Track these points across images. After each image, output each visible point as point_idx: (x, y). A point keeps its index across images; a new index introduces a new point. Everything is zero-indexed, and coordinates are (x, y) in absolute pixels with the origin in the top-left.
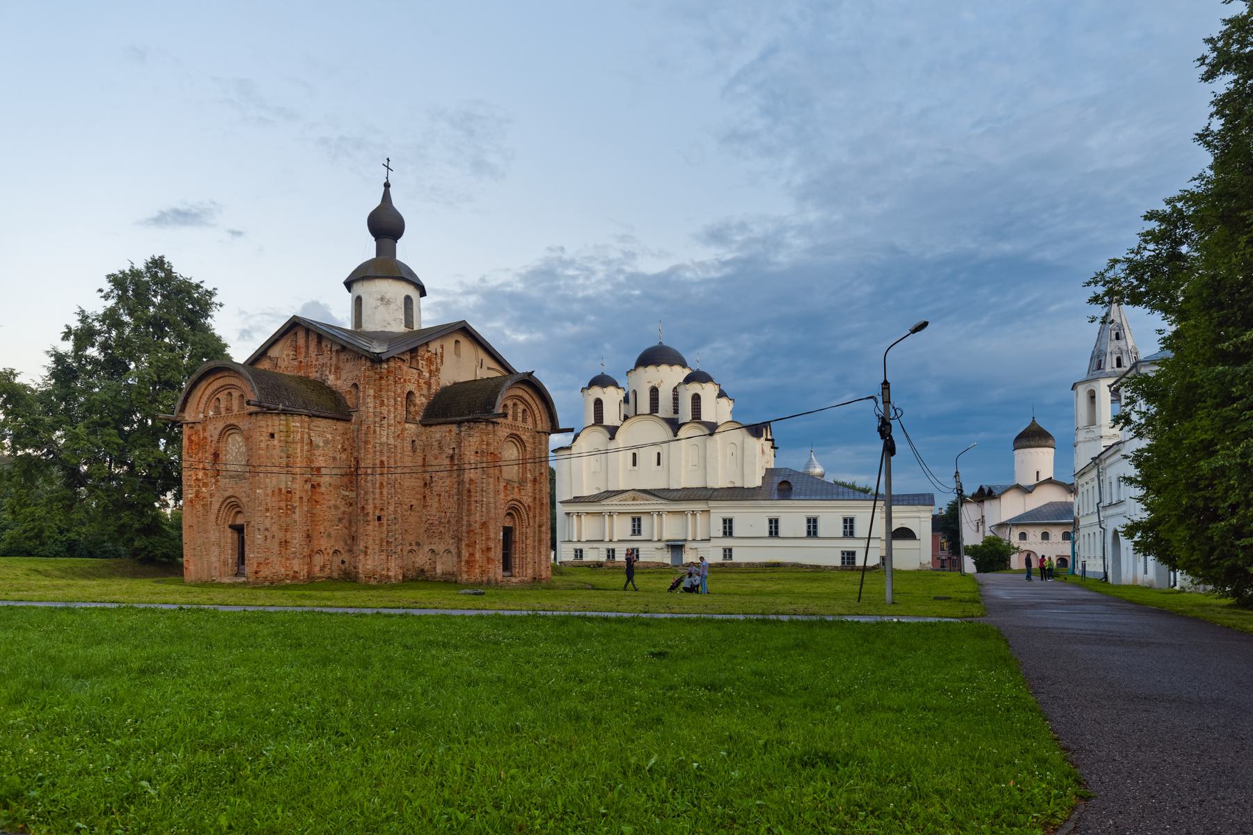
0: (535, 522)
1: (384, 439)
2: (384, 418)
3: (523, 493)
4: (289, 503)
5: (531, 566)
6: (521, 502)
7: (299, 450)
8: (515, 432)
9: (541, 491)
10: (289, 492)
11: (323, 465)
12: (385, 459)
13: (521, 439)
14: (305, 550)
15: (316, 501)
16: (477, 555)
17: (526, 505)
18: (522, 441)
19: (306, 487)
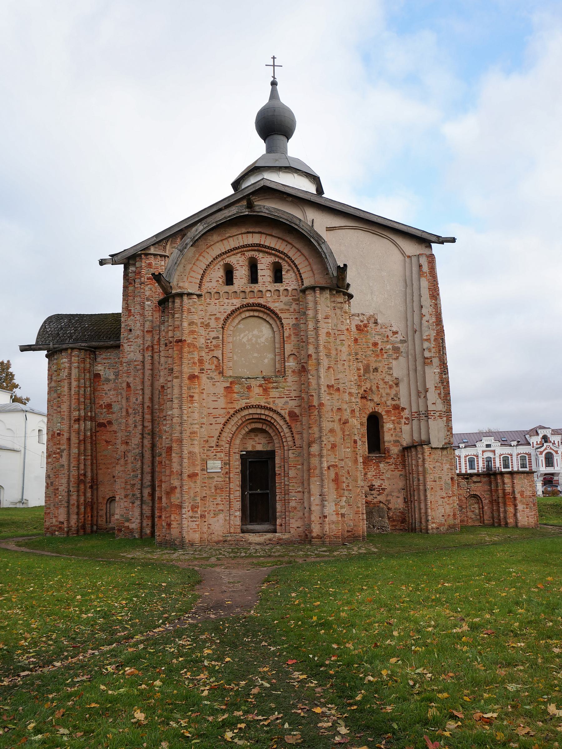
0: (302, 438)
1: (131, 356)
2: (131, 330)
3: (274, 393)
4: (58, 446)
5: (300, 514)
6: (270, 409)
7: (66, 389)
8: (251, 301)
9: (309, 383)
10: (59, 434)
11: (114, 399)
12: (130, 380)
13: (269, 309)
14: (74, 497)
15: (107, 442)
16: (164, 500)
17: (282, 412)
18: (273, 312)
19: (76, 426)
